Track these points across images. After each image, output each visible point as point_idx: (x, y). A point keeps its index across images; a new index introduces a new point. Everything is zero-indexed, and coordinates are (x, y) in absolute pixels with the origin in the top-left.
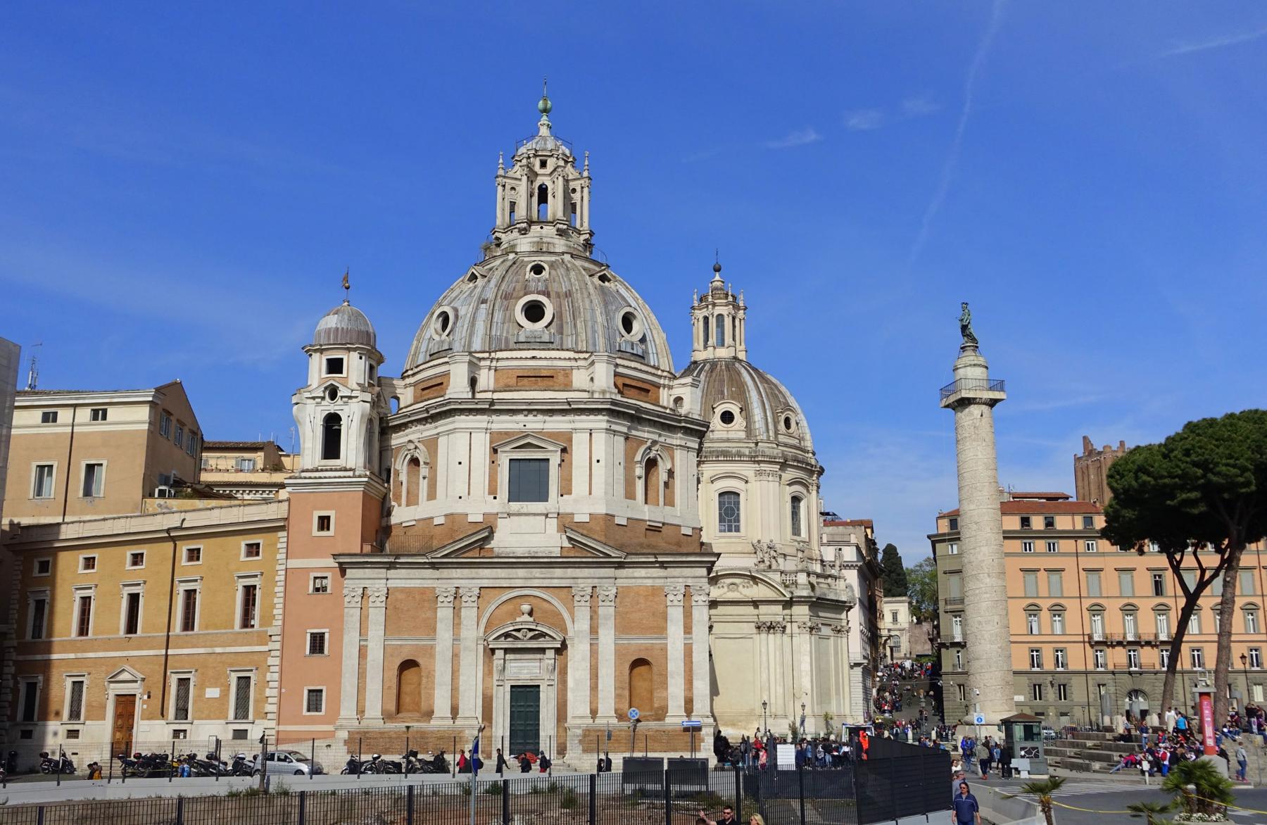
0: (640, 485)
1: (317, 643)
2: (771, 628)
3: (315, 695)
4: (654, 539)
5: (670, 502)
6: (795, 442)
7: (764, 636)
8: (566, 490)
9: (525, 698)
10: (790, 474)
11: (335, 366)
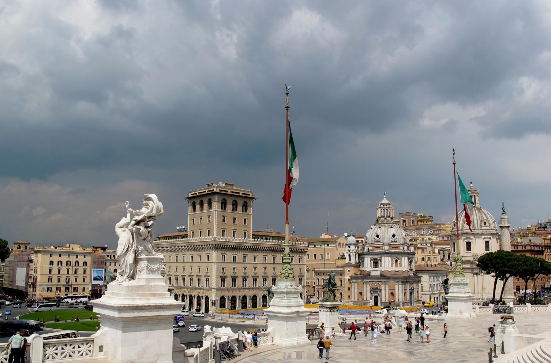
0: (394, 265)
1: (349, 288)
2: (477, 274)
3: (349, 296)
4: (397, 273)
5: (401, 266)
6: (488, 228)
7: (475, 276)
8: (381, 266)
9: (376, 298)
10: (483, 237)
11: (349, 247)
